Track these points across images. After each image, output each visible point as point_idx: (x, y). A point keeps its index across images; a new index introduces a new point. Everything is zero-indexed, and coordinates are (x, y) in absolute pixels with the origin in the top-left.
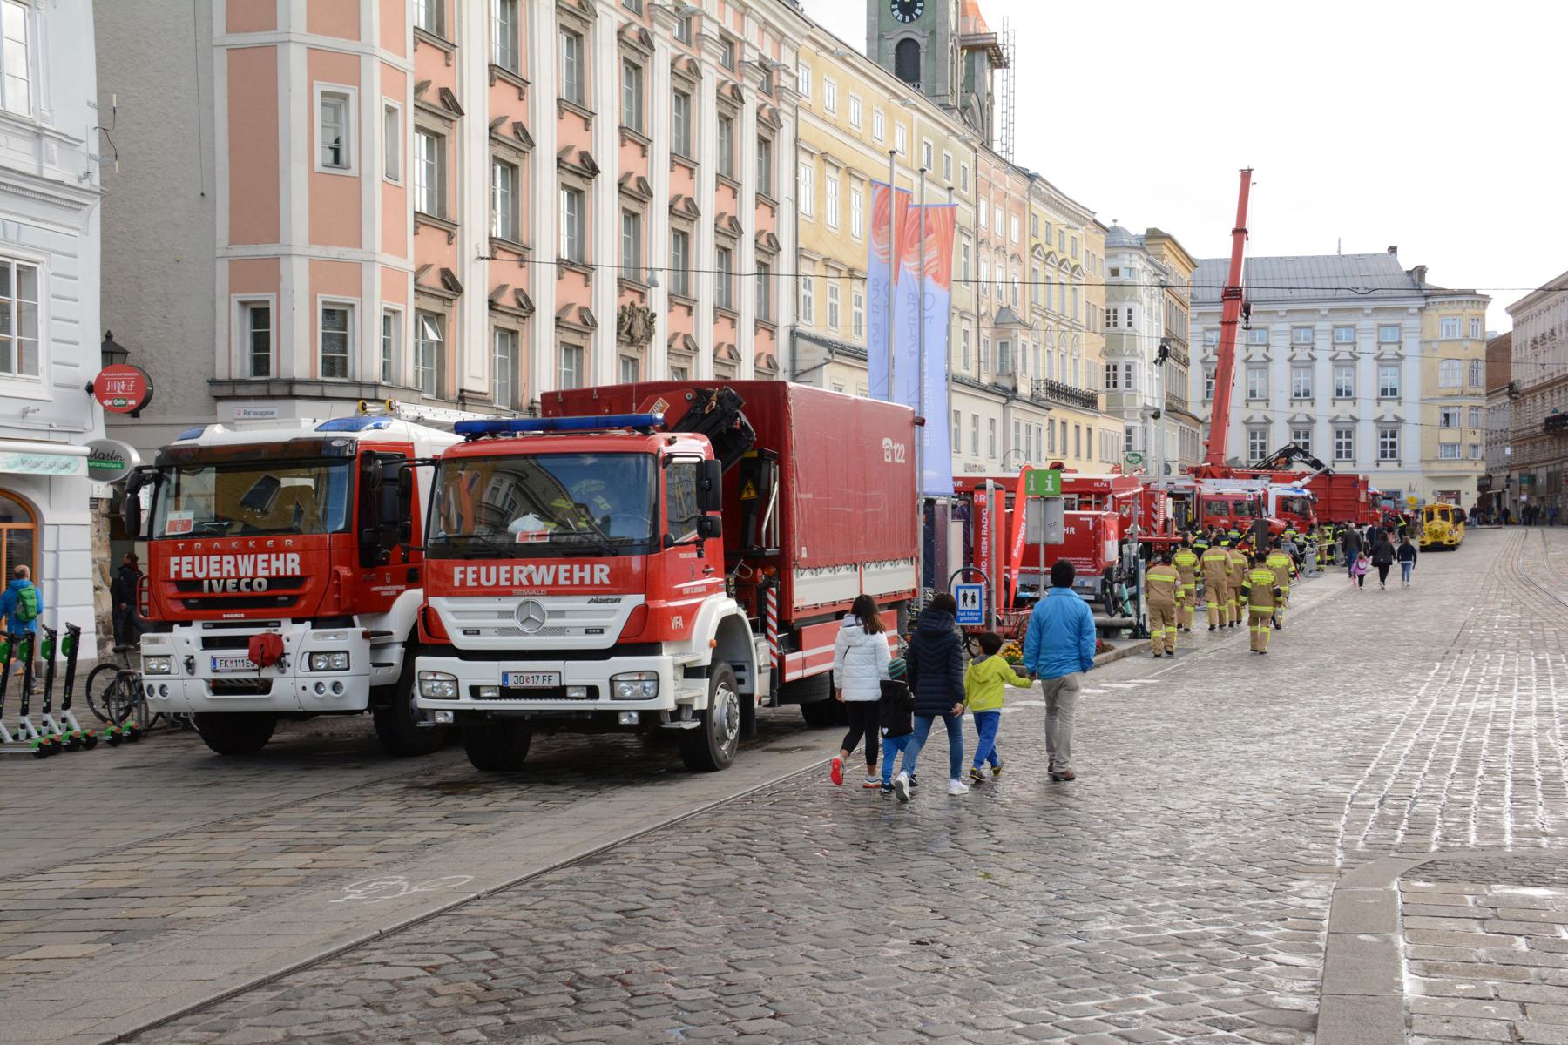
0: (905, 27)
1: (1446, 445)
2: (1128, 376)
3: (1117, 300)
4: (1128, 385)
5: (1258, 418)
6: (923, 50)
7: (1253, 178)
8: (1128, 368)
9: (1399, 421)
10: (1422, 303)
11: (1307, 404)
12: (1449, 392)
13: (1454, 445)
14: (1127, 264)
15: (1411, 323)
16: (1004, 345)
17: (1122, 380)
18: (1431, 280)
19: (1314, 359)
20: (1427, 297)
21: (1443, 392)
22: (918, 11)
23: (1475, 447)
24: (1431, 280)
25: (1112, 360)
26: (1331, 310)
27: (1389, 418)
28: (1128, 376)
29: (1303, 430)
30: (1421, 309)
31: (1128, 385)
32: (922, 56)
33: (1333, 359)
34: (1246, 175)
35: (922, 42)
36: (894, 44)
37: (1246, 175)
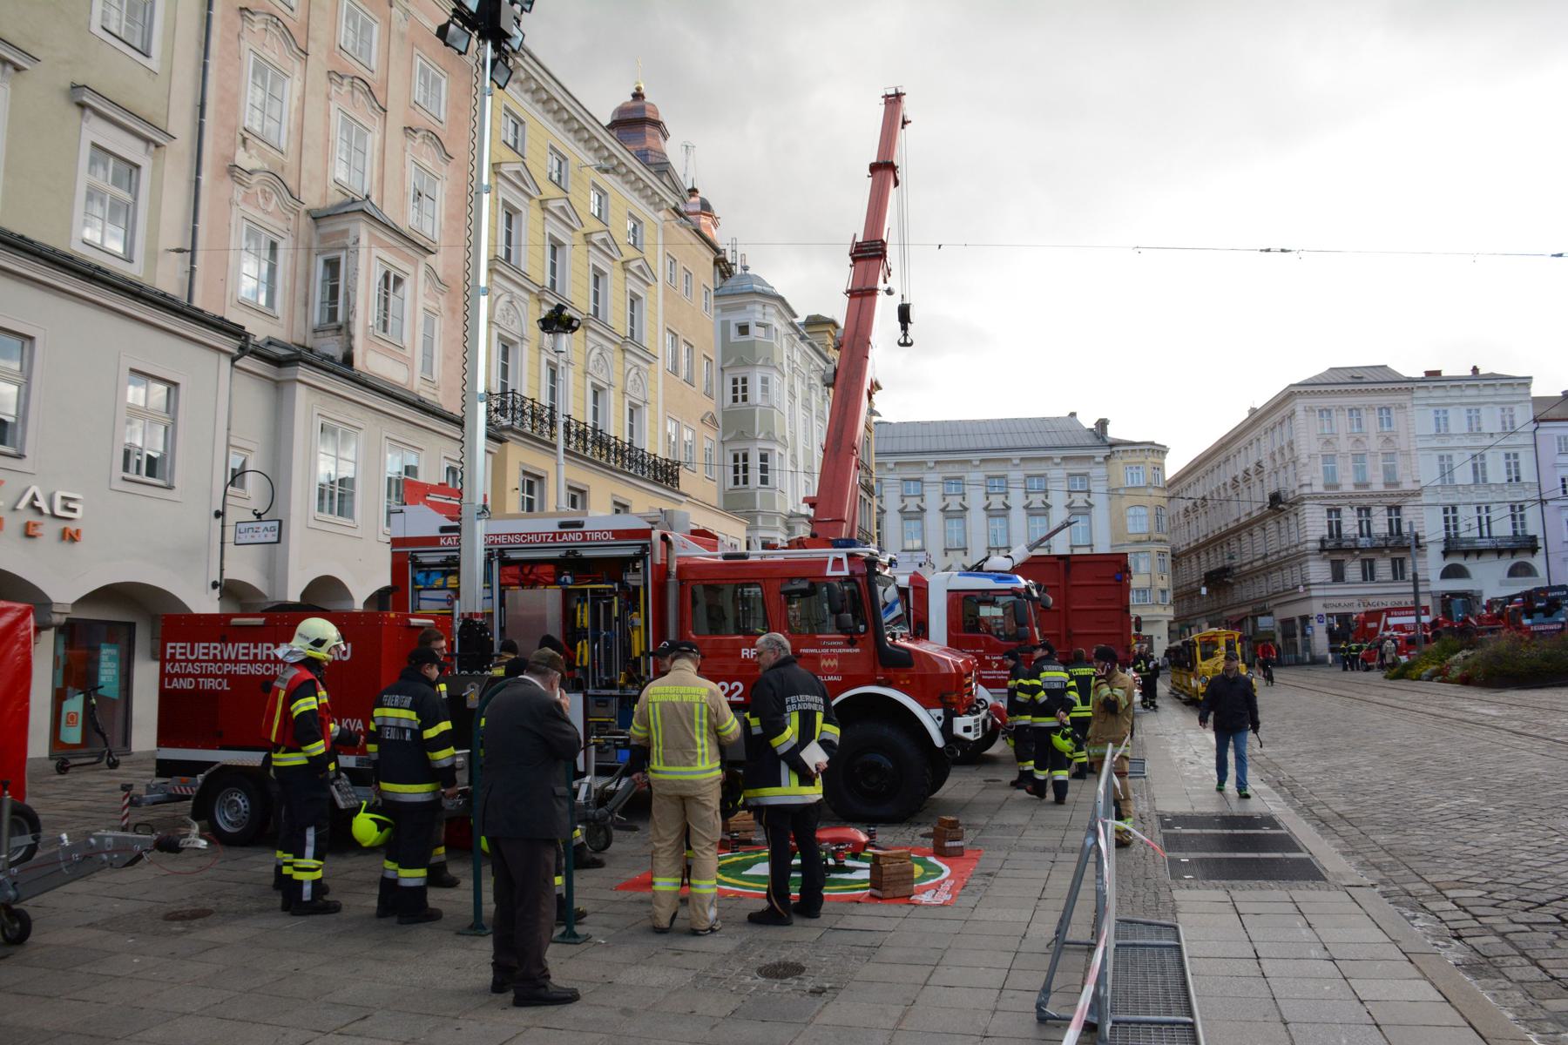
2: (764, 469)
3: (746, 365)
4: (764, 480)
7: (908, 108)
8: (764, 458)
10: (1107, 452)
12: (1137, 538)
13: (1144, 591)
14: (759, 318)
15: (1097, 472)
16: (333, 266)
17: (755, 475)
18: (1113, 433)
19: (1008, 508)
20: (1111, 446)
21: (1133, 538)
23: (1163, 592)
24: (1113, 433)
25: (740, 447)
26: (1022, 459)
28: (764, 469)
30: (1107, 458)
31: (764, 480)
33: (1026, 507)
34: (894, 100)
37: (894, 100)
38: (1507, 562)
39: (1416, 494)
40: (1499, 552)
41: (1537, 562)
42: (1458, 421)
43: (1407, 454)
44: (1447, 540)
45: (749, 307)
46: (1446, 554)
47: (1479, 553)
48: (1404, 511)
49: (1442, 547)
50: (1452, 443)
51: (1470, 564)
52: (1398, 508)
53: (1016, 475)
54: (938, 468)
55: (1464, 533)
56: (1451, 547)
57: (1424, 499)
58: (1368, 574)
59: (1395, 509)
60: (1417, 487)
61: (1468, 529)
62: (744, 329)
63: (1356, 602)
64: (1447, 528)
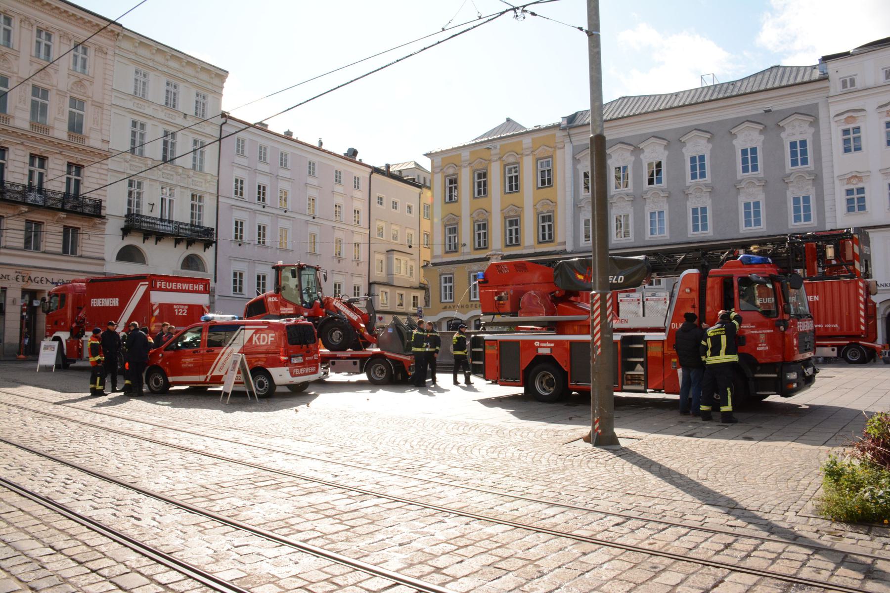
38: (182, 252)
39: (105, 156)
40: (178, 240)
41: (207, 256)
42: (157, 90)
43: (99, 106)
44: (129, 216)
46: (126, 231)
47: (160, 237)
48: (86, 172)
49: (122, 223)
50: (149, 111)
51: (149, 248)
52: (79, 168)
55: (145, 211)
56: (132, 224)
57: (111, 164)
58: (32, 240)
59: (76, 168)
60: (105, 147)
61: (149, 206)
63: (12, 273)
64: (129, 203)
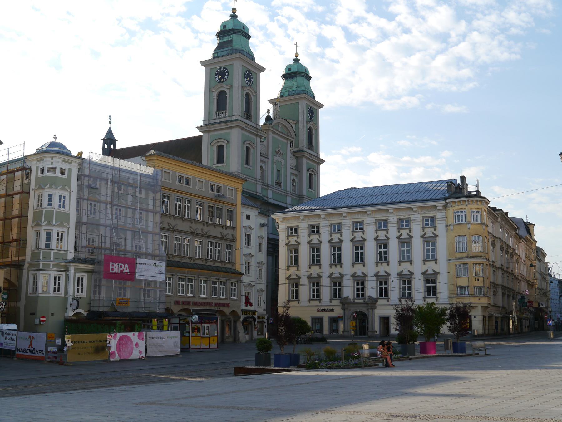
0: (221, 85)
1: (461, 288)
5: (359, 274)
6: (228, 95)
9: (436, 273)
10: (443, 203)
11: (385, 265)
12: (461, 255)
15: (440, 215)
21: (458, 255)
22: (226, 77)
27: (430, 272)
29: (383, 282)
32: (227, 98)
35: (228, 91)
36: (215, 94)
45: (45, 159)
53: (392, 219)
54: (349, 217)
62: (42, 170)
